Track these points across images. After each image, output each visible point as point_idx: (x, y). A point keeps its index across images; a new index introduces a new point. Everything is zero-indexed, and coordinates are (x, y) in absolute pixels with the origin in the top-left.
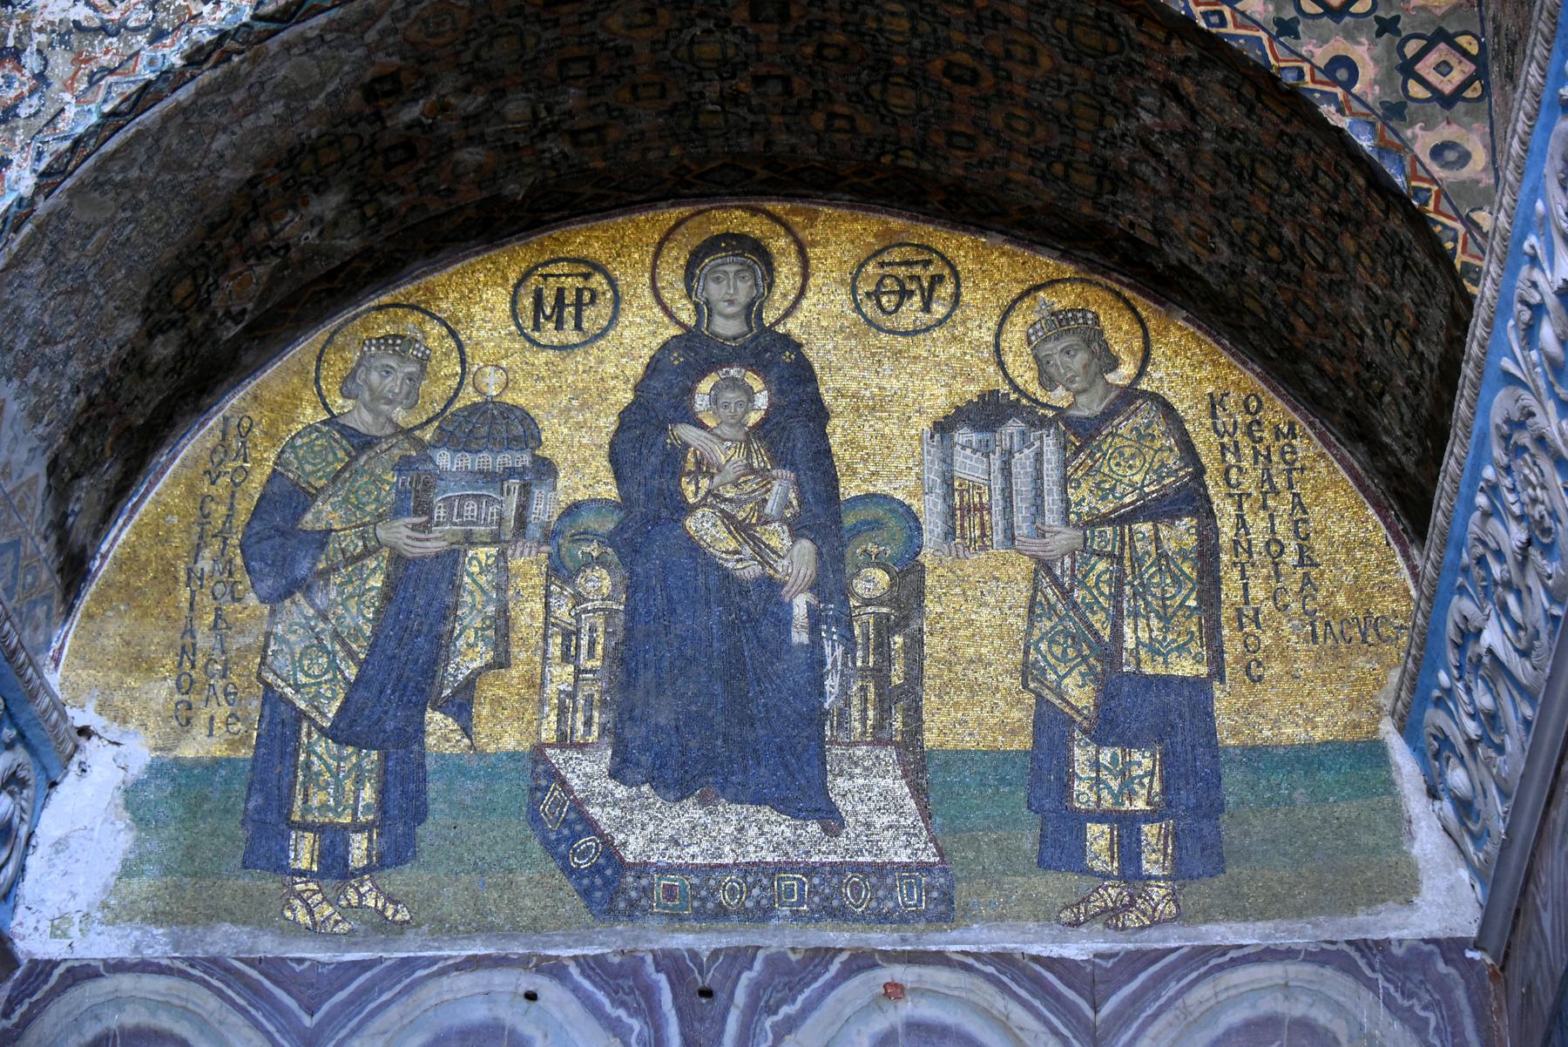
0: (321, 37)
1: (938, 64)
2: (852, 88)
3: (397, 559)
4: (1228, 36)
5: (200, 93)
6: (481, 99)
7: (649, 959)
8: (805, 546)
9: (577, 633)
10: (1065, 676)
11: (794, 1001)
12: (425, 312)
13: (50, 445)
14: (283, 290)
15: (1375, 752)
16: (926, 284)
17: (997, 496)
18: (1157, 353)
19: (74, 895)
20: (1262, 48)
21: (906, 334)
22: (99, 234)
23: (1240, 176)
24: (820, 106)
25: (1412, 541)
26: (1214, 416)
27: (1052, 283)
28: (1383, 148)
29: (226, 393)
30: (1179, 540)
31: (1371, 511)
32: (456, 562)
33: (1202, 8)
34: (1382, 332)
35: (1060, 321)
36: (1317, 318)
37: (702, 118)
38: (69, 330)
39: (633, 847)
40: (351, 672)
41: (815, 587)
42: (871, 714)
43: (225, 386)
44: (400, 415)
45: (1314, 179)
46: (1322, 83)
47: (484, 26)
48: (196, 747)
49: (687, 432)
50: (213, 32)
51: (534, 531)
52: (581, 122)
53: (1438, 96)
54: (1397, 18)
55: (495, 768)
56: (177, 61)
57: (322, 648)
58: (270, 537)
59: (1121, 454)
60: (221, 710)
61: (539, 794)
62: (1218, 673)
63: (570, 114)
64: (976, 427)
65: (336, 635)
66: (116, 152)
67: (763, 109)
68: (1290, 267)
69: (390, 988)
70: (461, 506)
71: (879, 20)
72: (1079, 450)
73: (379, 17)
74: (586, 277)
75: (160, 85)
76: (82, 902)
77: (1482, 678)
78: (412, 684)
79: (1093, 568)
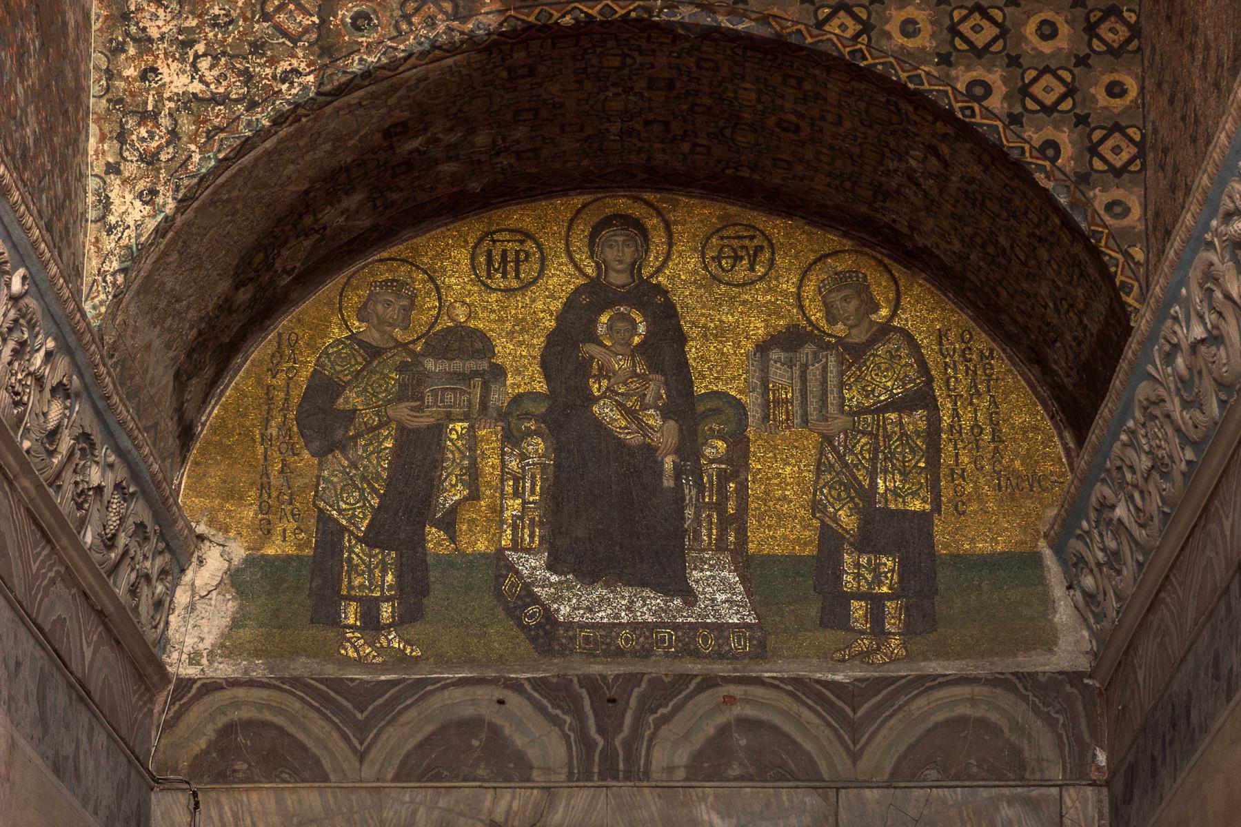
0: (360, 103)
5: (279, 142)
9: (523, 478)
20: (999, 133)
22: (211, 232)
30: (915, 424)
32: (441, 431)
33: (960, 104)
34: (1060, 308)
38: (190, 292)
40: (375, 502)
41: (678, 451)
45: (1025, 214)
46: (1037, 158)
53: (1112, 168)
54: (1088, 115)
56: (266, 123)
57: (356, 486)
60: (291, 525)
65: (364, 478)
66: (227, 181)
73: (399, 89)
77: (1112, 531)
78: (415, 510)
79: (859, 441)
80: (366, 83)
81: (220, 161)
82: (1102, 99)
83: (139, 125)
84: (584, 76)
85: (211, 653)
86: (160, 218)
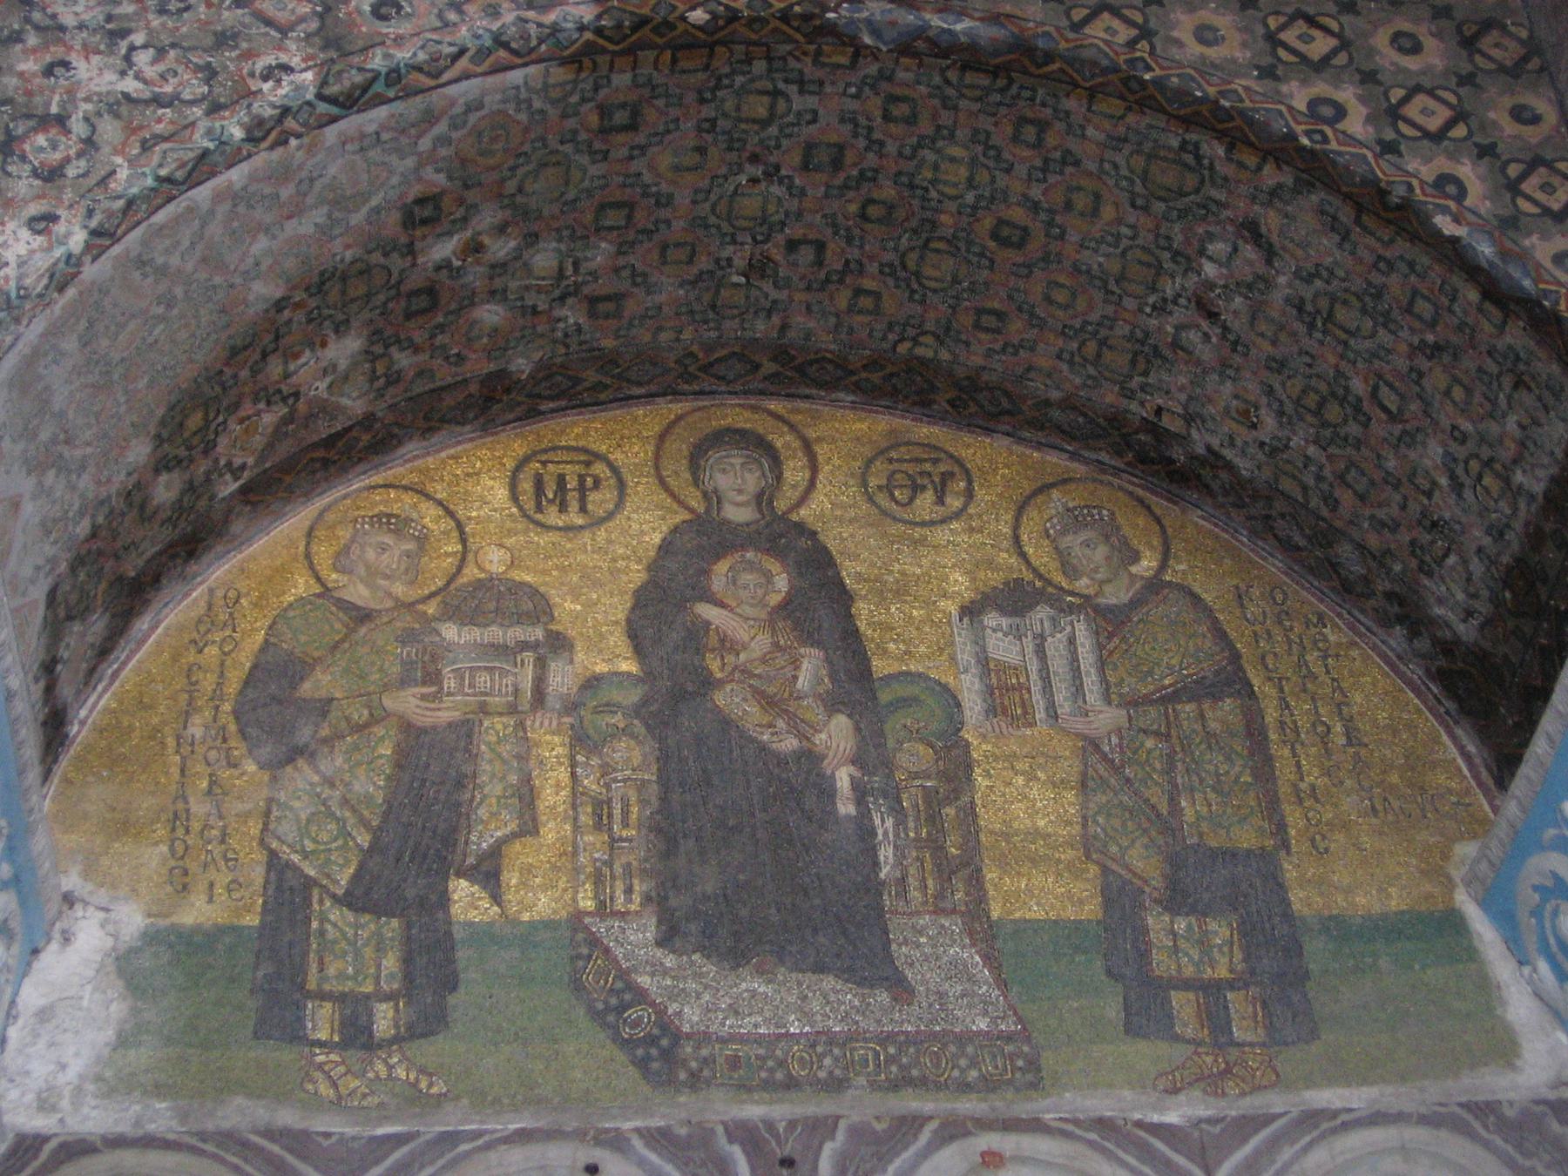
0: (377, 133)
1: (988, 223)
2: (890, 257)
3: (407, 727)
4: (1332, 151)
5: (253, 178)
6: (512, 244)
7: (720, 1130)
8: (841, 722)
9: (610, 800)
10: (1127, 848)
11: (885, 1170)
12: (418, 492)
13: (53, 569)
14: (285, 449)
15: (1453, 923)
16: (937, 480)
17: (1034, 677)
18: (1177, 546)
19: (63, 1067)
20: (1368, 164)
21: (923, 524)
22: (132, 326)
23: (1311, 326)
24: (848, 281)
25: (1457, 722)
26: (1242, 606)
27: (1065, 481)
28: (1504, 254)
29: (209, 566)
31: (1411, 695)
32: (469, 736)
34: (1463, 478)
35: (1076, 517)
36: (1372, 483)
37: (724, 293)
39: (690, 1016)
40: (364, 839)
41: (857, 761)
42: (930, 882)
43: (212, 555)
44: (399, 589)
45: (1409, 310)
47: (534, 149)
48: (197, 912)
49: (707, 611)
50: (275, 107)
51: (553, 702)
52: (603, 286)
55: (529, 936)
57: (333, 814)
58: (265, 705)
59: (1155, 640)
61: (581, 963)
62: (1286, 845)
63: (594, 274)
64: (1003, 611)
65: (345, 802)
66: (162, 228)
67: (788, 283)
68: (1354, 429)
69: (431, 1163)
70: (472, 677)
71: (936, 167)
72: (1111, 636)
73: (438, 120)
74: (588, 464)
75: (217, 158)
76: (71, 1074)
80: (391, 94)
81: (160, 180)
82: (1510, 127)
83: (35, 130)
84: (709, 138)
85: (78, 1091)
86: (59, 252)
